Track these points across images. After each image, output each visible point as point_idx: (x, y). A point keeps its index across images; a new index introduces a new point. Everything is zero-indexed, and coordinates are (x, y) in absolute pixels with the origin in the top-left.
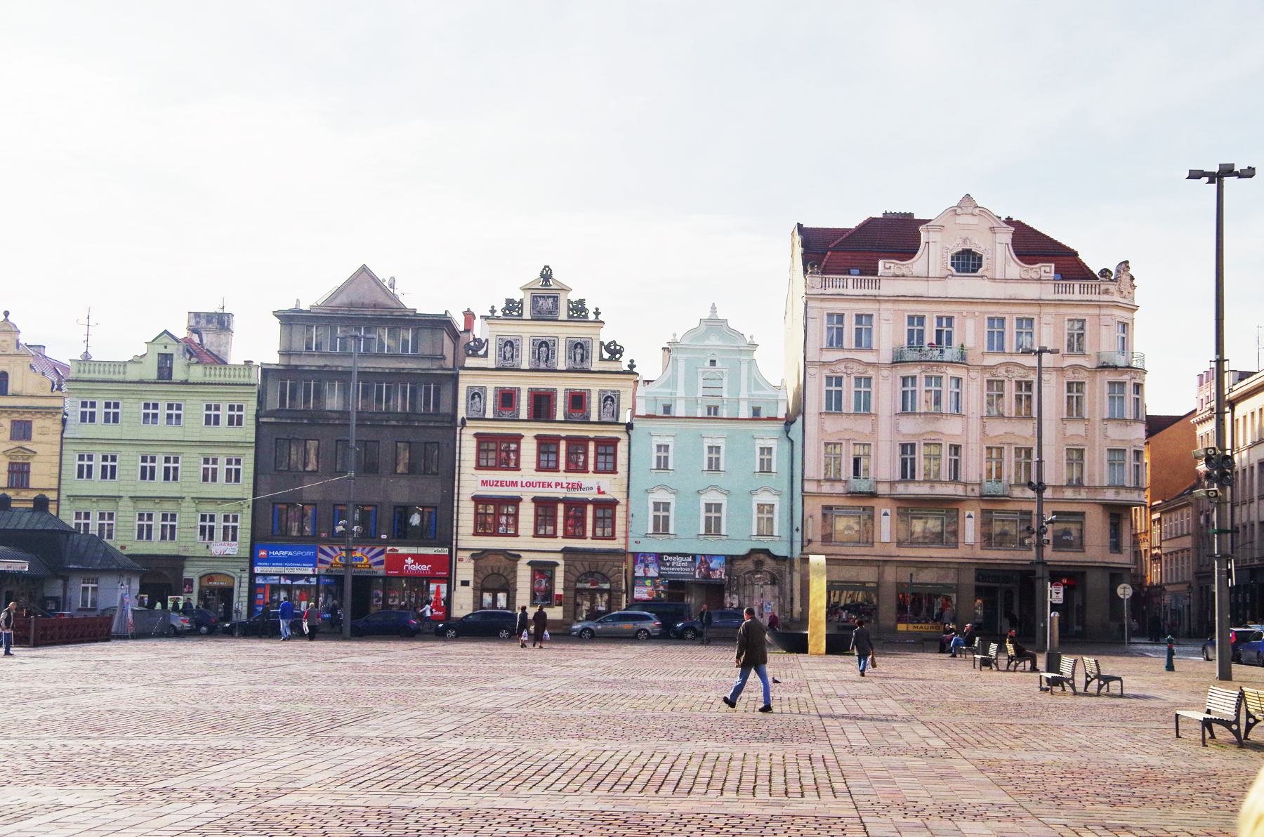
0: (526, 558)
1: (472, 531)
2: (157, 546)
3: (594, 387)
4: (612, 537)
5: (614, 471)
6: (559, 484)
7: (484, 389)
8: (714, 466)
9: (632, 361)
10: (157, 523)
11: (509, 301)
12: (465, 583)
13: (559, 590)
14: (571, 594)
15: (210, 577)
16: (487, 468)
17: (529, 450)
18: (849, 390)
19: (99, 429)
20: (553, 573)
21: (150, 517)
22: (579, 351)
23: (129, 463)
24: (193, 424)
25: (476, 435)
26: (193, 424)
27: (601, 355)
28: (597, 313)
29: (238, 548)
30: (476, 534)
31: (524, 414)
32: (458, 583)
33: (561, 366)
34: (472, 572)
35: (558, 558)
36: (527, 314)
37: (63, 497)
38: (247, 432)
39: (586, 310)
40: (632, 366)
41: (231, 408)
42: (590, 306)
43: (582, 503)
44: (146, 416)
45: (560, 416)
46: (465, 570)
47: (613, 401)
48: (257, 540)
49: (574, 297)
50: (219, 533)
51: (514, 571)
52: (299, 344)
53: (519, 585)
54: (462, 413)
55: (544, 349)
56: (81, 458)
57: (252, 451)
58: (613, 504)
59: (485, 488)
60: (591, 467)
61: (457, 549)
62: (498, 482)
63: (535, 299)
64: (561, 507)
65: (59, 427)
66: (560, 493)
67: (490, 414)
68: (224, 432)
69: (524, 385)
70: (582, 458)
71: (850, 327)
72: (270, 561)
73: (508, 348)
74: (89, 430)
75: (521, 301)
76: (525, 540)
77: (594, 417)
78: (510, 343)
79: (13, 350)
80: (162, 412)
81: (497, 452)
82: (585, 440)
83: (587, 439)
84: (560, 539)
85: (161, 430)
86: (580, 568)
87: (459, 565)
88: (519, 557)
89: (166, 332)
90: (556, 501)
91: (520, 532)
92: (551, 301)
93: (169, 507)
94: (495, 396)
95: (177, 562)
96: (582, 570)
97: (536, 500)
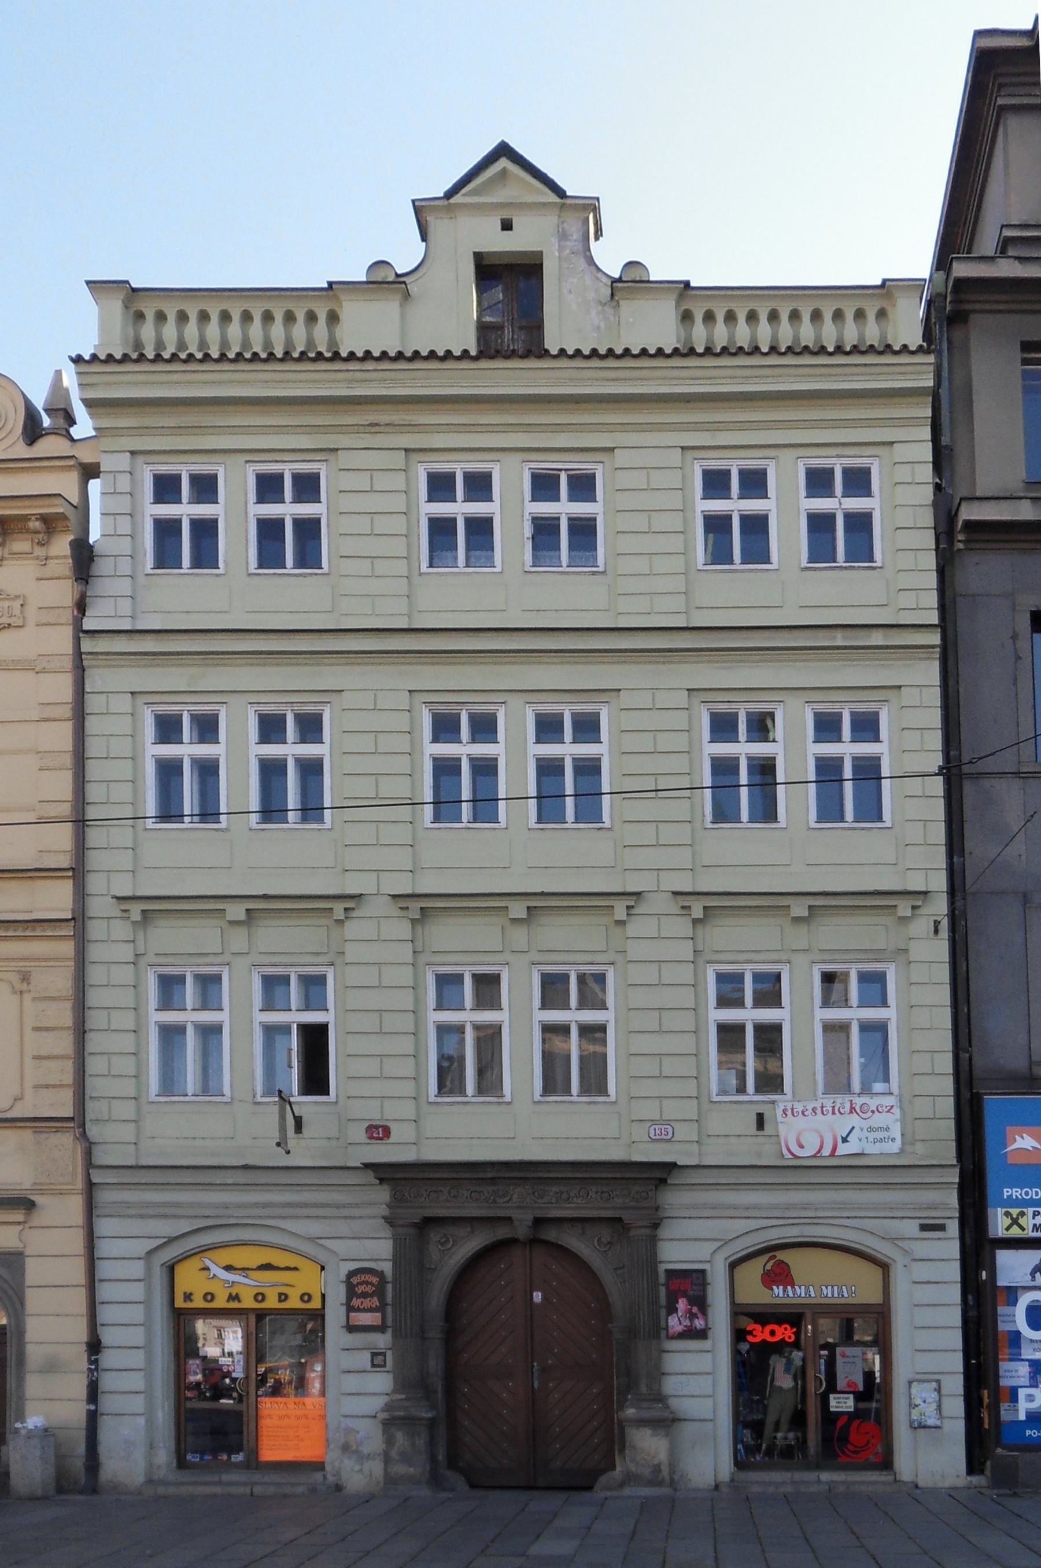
2: (521, 1124)
10: (520, 1019)
15: (775, 1261)
19: (238, 590)
21: (487, 987)
23: (375, 737)
24: (651, 546)
26: (651, 546)
37: (99, 906)
38: (903, 579)
41: (819, 482)
44: (441, 530)
50: (802, 1055)
56: (168, 729)
57: (930, 672)
65: (65, 592)
68: (788, 585)
74: (184, 597)
80: (512, 509)
85: (509, 587)
89: (503, 150)
93: (572, 943)
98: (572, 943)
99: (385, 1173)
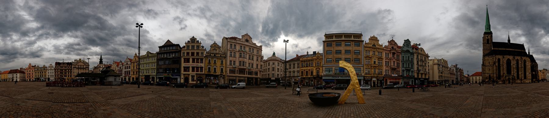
3: (200, 52)
6: (195, 65)
8: (215, 62)
17: (191, 60)
18: (233, 54)
46: (182, 77)
62: (187, 65)
69: (190, 52)
71: (233, 46)
76: (190, 72)
81: (187, 61)
82: (198, 59)
86: (198, 76)
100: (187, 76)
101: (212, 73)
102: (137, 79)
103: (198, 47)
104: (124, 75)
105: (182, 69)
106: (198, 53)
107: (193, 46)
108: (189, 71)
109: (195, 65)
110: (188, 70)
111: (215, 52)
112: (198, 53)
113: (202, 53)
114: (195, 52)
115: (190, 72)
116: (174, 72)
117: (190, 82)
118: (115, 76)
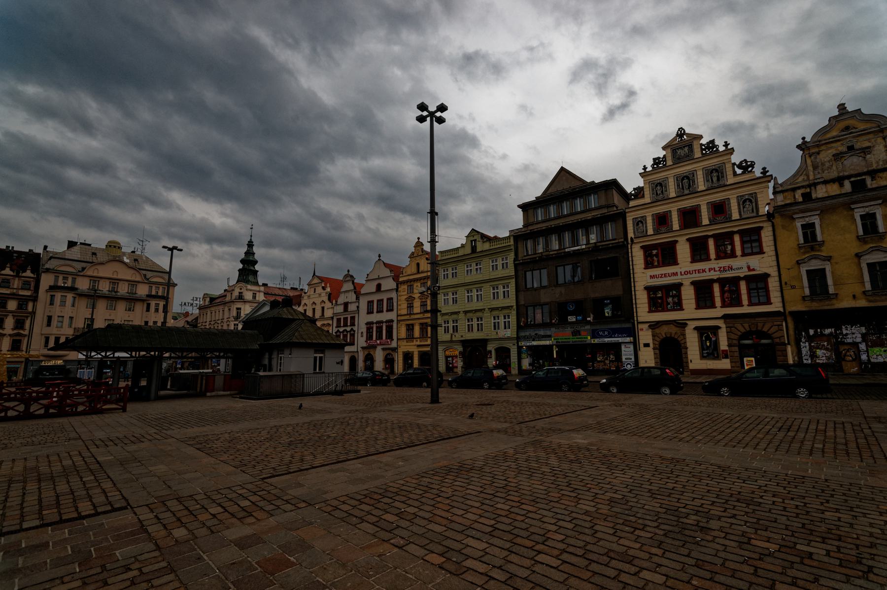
0: (692, 325)
1: (647, 310)
2: (475, 335)
4: (768, 302)
5: (761, 252)
6: (712, 268)
7: (644, 218)
9: (764, 169)
11: (654, 159)
12: (646, 345)
13: (724, 345)
14: (736, 349)
16: (653, 267)
17: (683, 251)
20: (716, 334)
22: (715, 174)
25: (642, 247)
27: (735, 174)
28: (726, 144)
29: (510, 333)
30: (650, 311)
31: (676, 226)
32: (641, 345)
33: (701, 187)
34: (651, 337)
35: (720, 323)
36: (669, 162)
39: (716, 146)
40: (764, 171)
42: (720, 144)
43: (736, 280)
45: (705, 221)
46: (645, 336)
47: (750, 201)
48: (519, 328)
49: (704, 141)
51: (684, 335)
52: (531, 220)
53: (688, 344)
54: (631, 234)
55: (686, 181)
58: (766, 276)
59: (652, 280)
60: (738, 252)
61: (638, 323)
62: (663, 275)
63: (674, 152)
64: (716, 288)
66: (714, 275)
67: (650, 231)
70: (729, 247)
72: (527, 338)
73: (659, 188)
75: (664, 156)
76: (689, 309)
77: (735, 215)
78: (660, 184)
79: (420, 253)
82: (729, 236)
83: (733, 233)
84: (719, 309)
86: (742, 327)
87: (641, 333)
88: (686, 324)
90: (712, 281)
91: (684, 306)
92: (686, 149)
94: (653, 219)
95: (484, 342)
96: (743, 330)
97: (695, 284)
98: (479, 314)
99: (461, 341)
100: (673, 330)
101: (846, 303)
102: (425, 358)
103: (716, 175)
104: (361, 341)
105: (641, 299)
106: (719, 210)
107: (686, 182)
108: (678, 306)
109: (712, 268)
110: (674, 299)
111: (853, 164)
112: (719, 210)
113: (748, 202)
114: (703, 204)
115: (689, 309)
116: (600, 317)
117: (695, 360)
118: (320, 348)
